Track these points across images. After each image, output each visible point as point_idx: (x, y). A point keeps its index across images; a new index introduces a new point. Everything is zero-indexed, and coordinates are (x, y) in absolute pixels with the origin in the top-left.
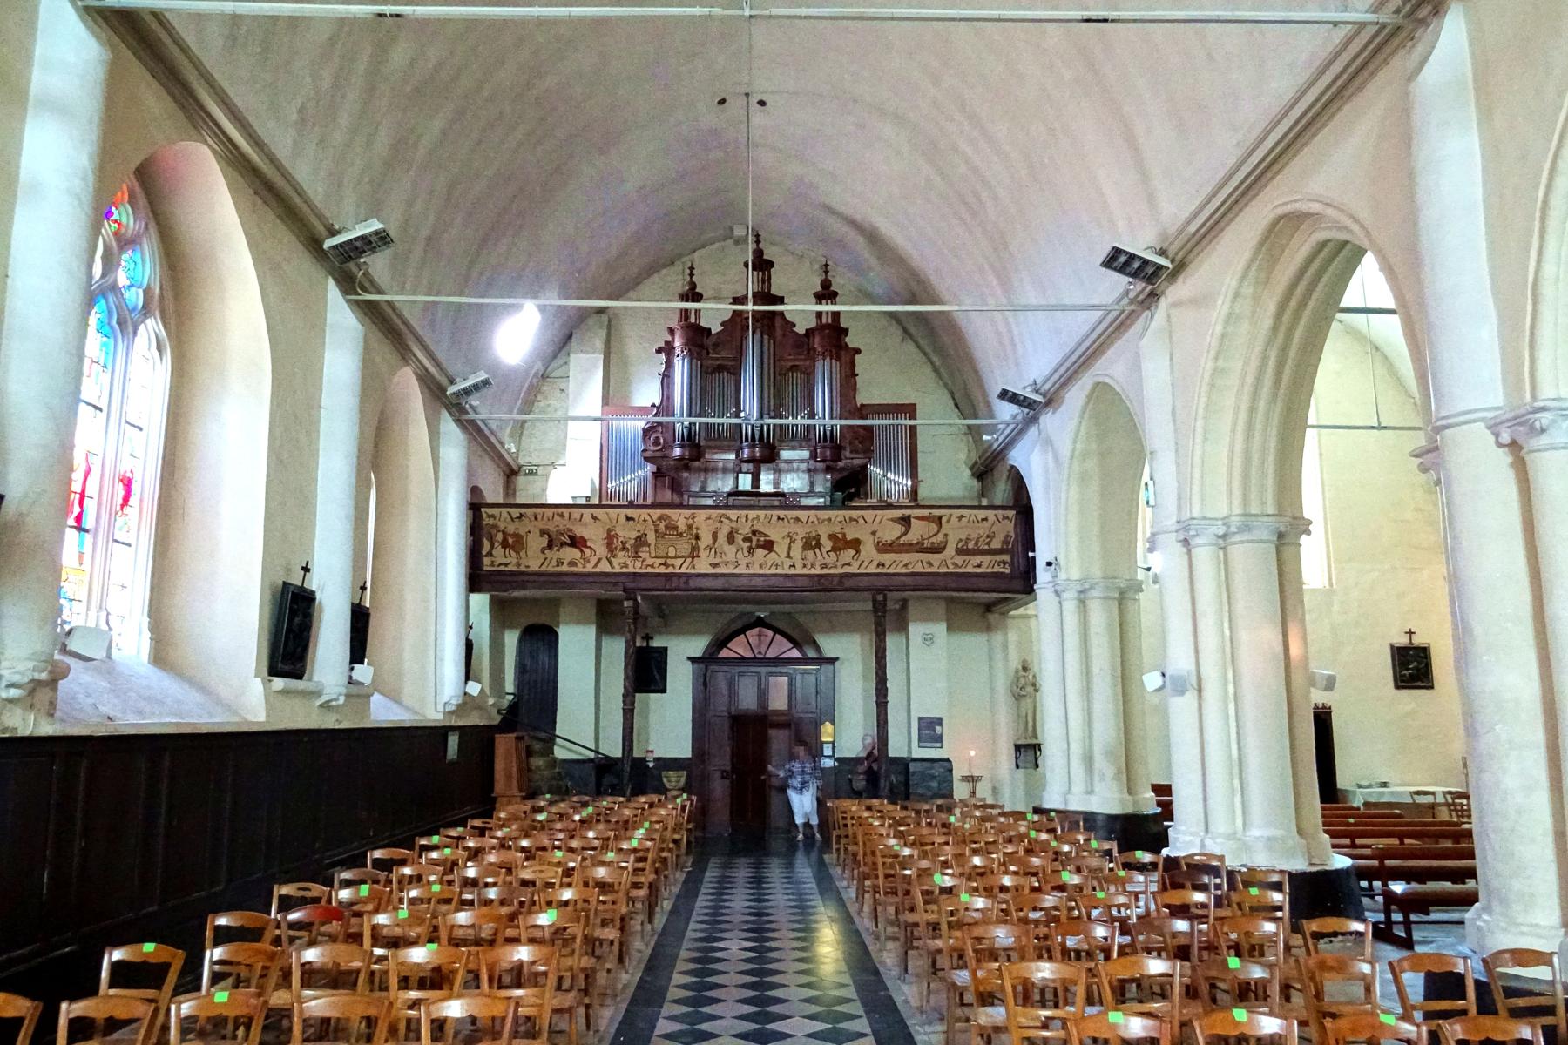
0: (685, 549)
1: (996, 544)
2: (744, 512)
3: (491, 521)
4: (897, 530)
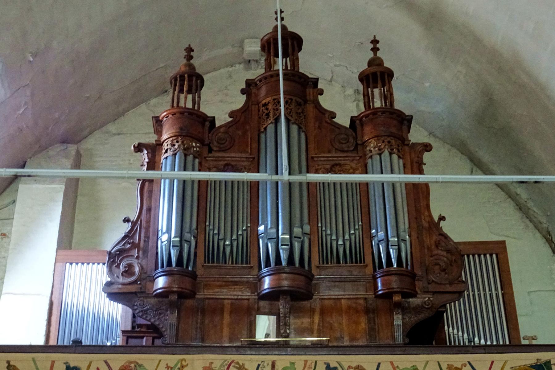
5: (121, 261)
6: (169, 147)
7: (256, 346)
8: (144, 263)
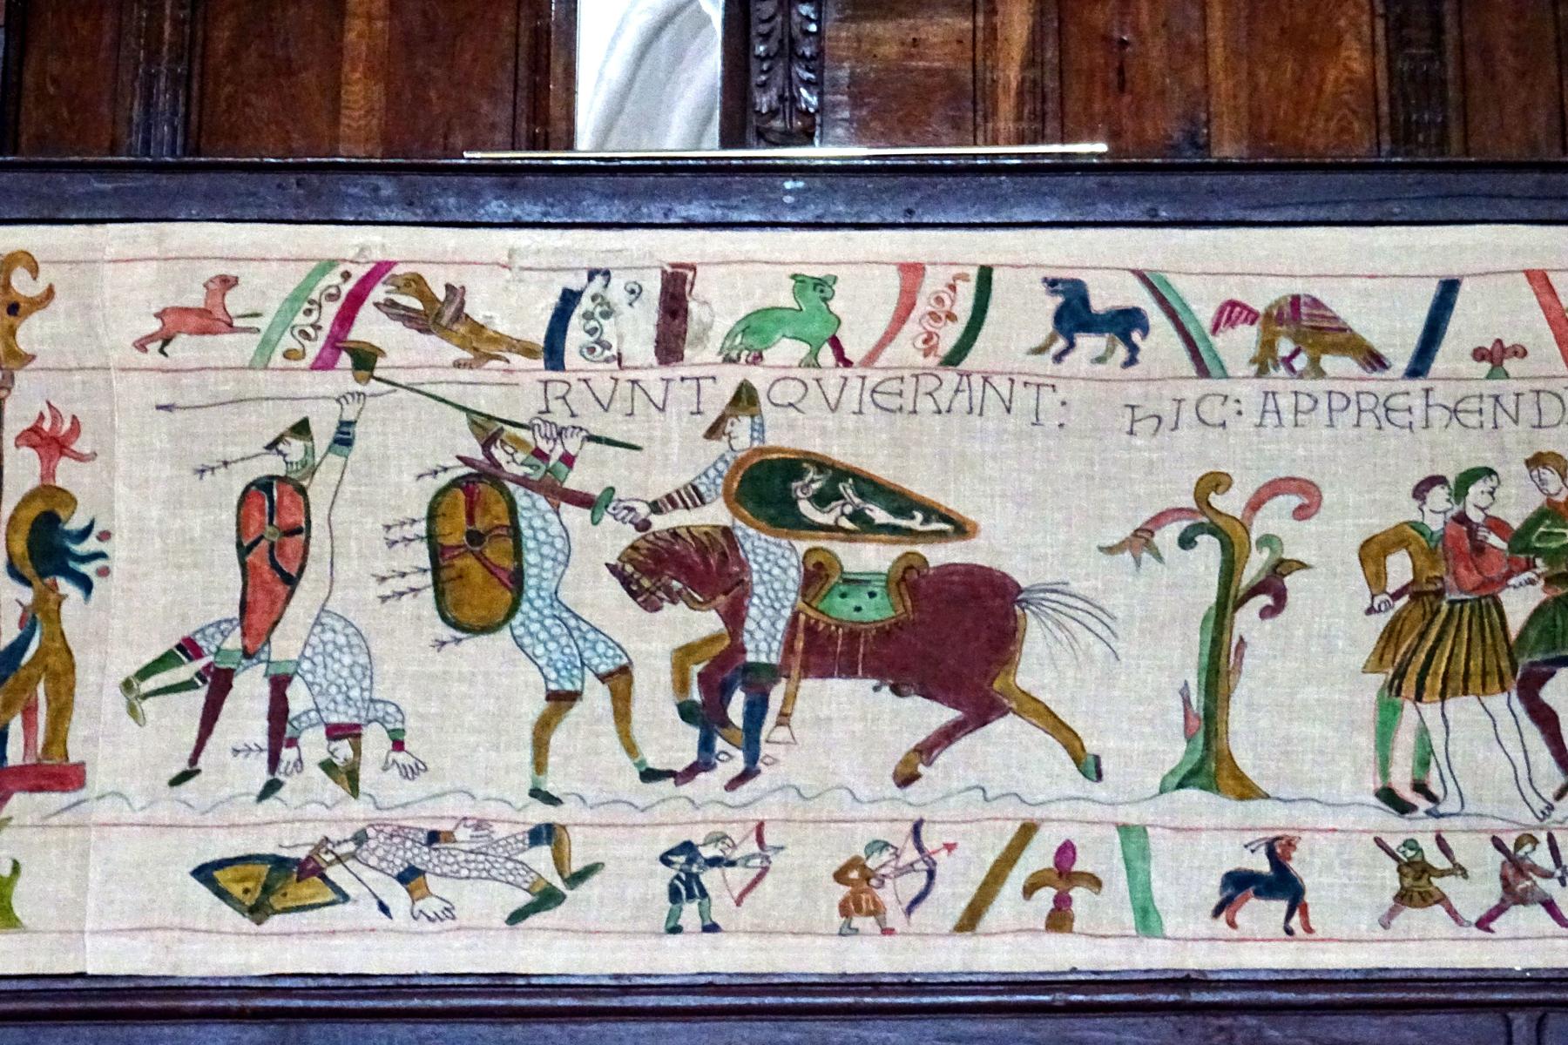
2: (643, 253)
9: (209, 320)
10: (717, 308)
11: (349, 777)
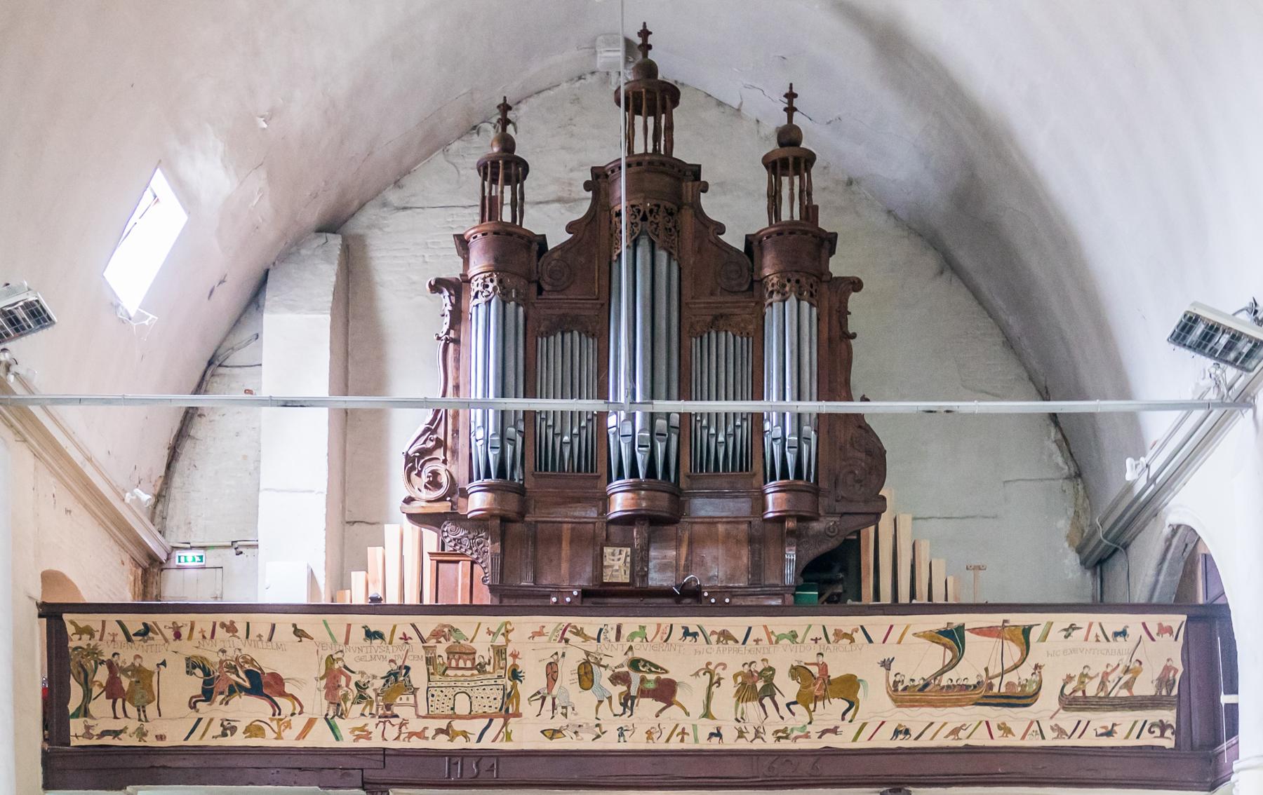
0: (490, 698)
1: (1145, 687)
3: (85, 641)
4: (937, 655)
5: (422, 466)
6: (480, 288)
7: (599, 597)
8: (453, 470)
9: (540, 634)
10: (625, 632)
11: (566, 715)
